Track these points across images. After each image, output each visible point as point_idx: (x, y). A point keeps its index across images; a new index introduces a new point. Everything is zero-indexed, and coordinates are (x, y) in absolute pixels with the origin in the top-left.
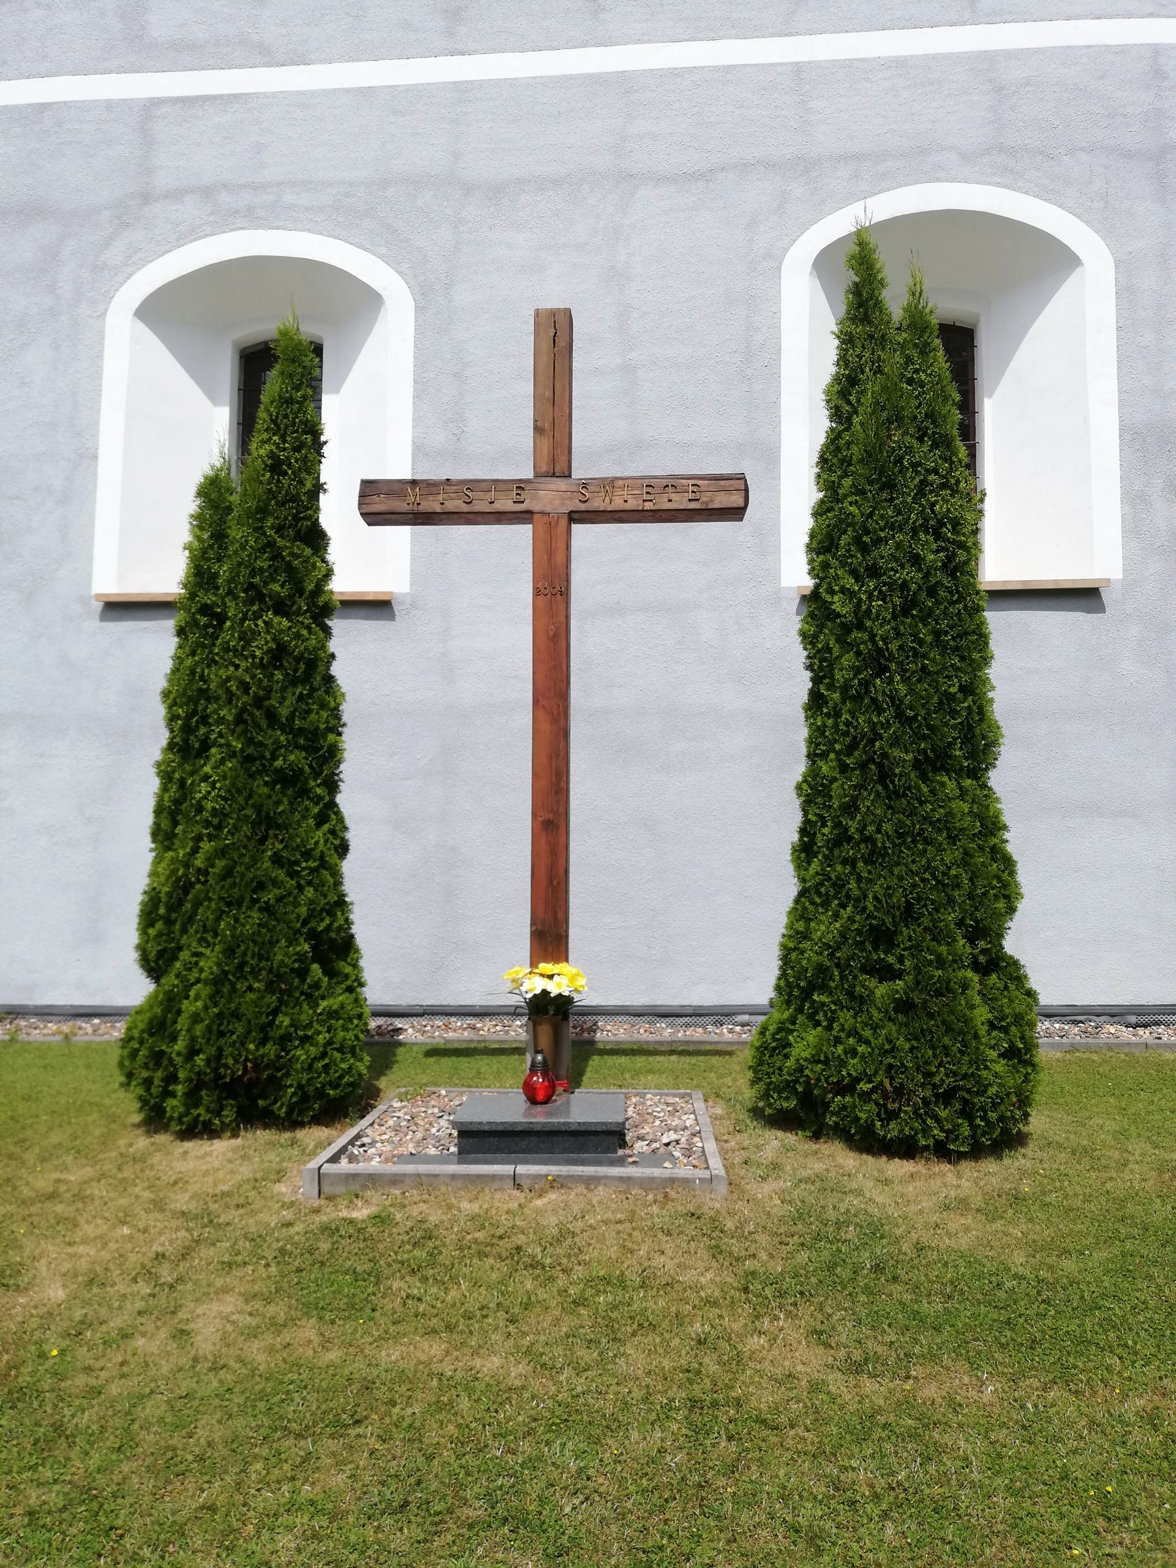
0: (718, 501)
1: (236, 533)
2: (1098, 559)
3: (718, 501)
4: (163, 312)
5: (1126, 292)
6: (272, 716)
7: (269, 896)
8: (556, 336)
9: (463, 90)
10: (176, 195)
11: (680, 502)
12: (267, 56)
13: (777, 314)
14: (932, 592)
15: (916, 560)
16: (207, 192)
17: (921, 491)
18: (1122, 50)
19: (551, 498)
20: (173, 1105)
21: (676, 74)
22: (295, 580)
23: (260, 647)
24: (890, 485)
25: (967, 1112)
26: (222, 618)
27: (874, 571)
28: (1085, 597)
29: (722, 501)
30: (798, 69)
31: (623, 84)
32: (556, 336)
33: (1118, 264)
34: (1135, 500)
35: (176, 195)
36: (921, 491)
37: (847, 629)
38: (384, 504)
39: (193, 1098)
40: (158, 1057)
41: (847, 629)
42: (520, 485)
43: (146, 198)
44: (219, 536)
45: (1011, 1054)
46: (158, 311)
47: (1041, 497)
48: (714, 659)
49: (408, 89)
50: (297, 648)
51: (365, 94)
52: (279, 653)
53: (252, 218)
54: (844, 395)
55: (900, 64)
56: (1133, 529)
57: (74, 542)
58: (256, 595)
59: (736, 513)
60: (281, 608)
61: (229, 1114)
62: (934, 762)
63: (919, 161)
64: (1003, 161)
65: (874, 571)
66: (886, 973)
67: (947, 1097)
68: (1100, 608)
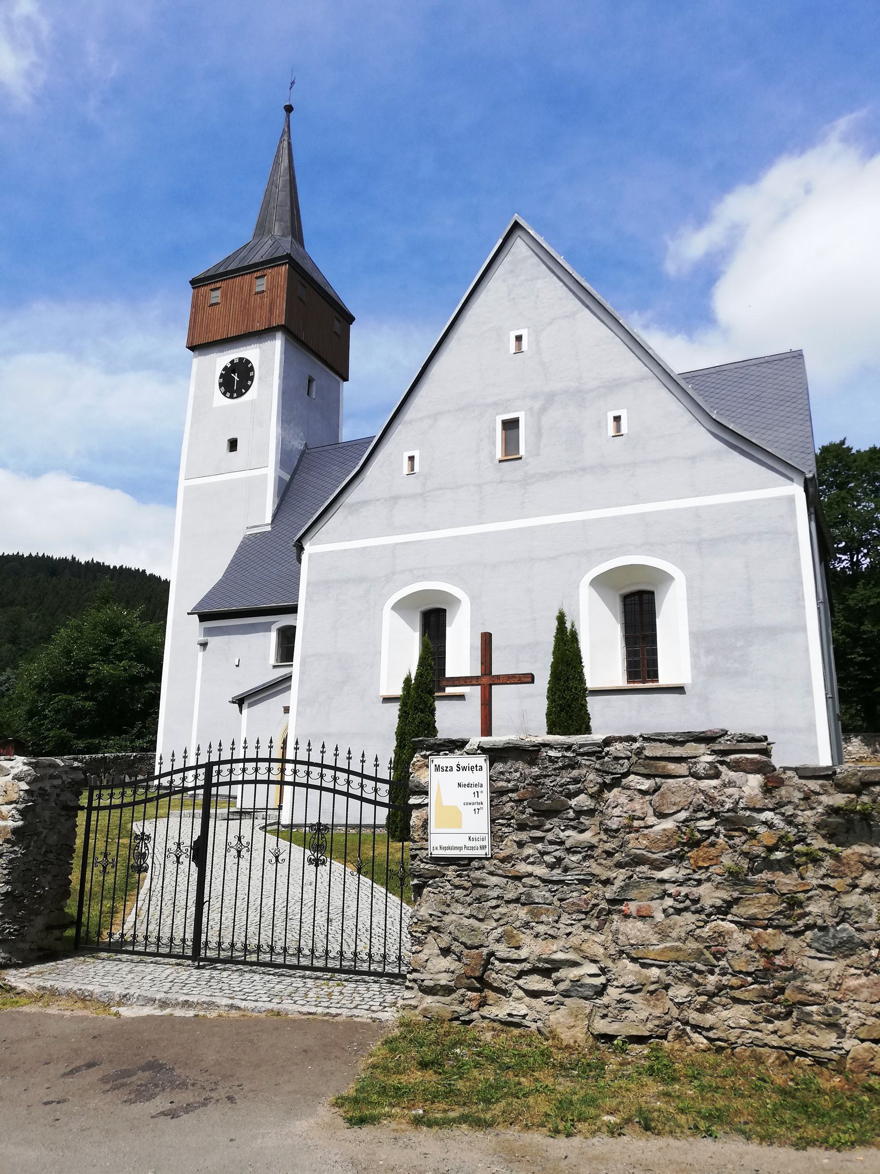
0: (529, 679)
1: (412, 693)
3: (529, 679)
4: (400, 607)
5: (690, 588)
9: (483, 535)
12: (427, 528)
13: (578, 600)
14: (569, 706)
15: (564, 698)
18: (686, 509)
19: (485, 680)
21: (547, 526)
22: (425, 704)
28: (679, 690)
31: (531, 530)
33: (687, 579)
34: (695, 656)
40: (394, 822)
42: (477, 677)
43: (394, 573)
44: (408, 693)
46: (398, 607)
50: (425, 721)
52: (421, 722)
56: (695, 666)
58: (416, 708)
59: (533, 682)
60: (422, 711)
63: (622, 550)
64: (649, 547)
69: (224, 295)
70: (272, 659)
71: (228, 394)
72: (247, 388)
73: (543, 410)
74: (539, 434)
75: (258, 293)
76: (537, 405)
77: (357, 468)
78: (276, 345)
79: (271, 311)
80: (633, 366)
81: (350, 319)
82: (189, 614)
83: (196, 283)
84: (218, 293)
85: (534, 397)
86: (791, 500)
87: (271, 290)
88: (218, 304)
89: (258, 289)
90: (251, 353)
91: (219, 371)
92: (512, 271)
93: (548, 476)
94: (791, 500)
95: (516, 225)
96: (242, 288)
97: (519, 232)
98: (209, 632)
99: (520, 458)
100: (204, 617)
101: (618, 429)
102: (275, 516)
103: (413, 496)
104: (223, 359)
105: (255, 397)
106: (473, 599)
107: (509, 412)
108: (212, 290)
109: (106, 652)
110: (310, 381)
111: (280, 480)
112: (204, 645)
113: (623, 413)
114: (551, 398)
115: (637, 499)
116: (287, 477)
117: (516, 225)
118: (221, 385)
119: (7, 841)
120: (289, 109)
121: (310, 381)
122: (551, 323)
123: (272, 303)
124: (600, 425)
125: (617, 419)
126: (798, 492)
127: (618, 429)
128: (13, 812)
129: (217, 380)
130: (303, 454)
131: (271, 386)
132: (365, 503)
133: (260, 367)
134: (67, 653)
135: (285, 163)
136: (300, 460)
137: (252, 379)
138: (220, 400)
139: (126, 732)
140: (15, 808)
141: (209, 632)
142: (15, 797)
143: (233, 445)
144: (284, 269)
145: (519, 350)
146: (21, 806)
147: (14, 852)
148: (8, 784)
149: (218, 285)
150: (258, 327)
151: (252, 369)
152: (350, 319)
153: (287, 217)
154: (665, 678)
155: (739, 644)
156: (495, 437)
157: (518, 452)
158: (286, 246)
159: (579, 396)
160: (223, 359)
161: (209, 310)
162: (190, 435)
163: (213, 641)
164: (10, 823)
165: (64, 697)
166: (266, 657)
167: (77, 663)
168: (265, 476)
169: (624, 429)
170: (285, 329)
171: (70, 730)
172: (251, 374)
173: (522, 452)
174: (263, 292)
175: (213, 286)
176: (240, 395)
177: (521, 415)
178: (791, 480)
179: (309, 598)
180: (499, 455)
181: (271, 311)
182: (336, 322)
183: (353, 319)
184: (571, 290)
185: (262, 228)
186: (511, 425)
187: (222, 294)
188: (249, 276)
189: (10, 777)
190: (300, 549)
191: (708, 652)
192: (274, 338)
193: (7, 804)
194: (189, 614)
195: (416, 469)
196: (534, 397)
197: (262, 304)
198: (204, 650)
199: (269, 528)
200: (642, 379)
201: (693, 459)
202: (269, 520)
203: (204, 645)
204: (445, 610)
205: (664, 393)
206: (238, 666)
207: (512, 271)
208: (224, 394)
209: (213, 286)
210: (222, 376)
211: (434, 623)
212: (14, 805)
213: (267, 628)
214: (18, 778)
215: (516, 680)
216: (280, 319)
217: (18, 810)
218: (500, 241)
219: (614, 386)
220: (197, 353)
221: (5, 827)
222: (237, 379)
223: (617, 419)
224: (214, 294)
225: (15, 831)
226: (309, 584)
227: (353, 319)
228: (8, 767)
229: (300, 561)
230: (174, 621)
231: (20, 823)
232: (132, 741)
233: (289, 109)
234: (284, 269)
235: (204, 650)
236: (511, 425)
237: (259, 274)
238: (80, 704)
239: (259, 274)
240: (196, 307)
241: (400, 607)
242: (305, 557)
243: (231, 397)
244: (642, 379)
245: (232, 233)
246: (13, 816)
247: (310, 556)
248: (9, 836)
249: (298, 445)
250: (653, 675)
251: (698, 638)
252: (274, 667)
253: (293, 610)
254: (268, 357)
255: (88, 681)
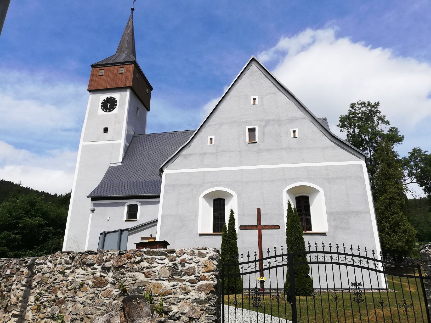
0: (277, 227)
2: (324, 229)
3: (277, 227)
4: (206, 197)
5: (326, 196)
6: (233, 251)
7: (233, 269)
8: (259, 210)
9: (242, 170)
10: (207, 183)
11: (273, 228)
15: (296, 235)
16: (211, 182)
17: (296, 228)
20: (225, 291)
21: (268, 169)
23: (231, 243)
24: (293, 228)
25: (304, 291)
26: (227, 240)
27: (292, 236)
28: (324, 234)
29: (277, 228)
30: (283, 168)
32: (259, 210)
34: (329, 221)
35: (207, 183)
36: (296, 228)
37: (290, 242)
38: (242, 228)
39: (227, 290)
41: (290, 242)
42: (256, 226)
43: (204, 183)
45: (309, 286)
46: (205, 197)
47: (319, 219)
48: (277, 241)
49: (235, 170)
51: (230, 171)
53: (217, 186)
54: (288, 217)
55: (295, 168)
56: (329, 225)
57: (196, 226)
61: (231, 292)
62: (300, 255)
65: (292, 236)
66: (296, 277)
67: (302, 289)
68: (326, 235)
69: (106, 72)
70: (125, 217)
71: (105, 110)
72: (114, 109)
73: (265, 126)
74: (264, 134)
75: (120, 73)
76: (263, 124)
77: (188, 141)
78: (127, 94)
79: (126, 81)
80: (299, 113)
81: (151, 89)
82: (87, 197)
83: (93, 66)
84: (103, 71)
85: (261, 121)
86: (361, 166)
87: (126, 73)
88: (102, 75)
89: (121, 72)
90: (116, 96)
91: (101, 100)
92: (251, 75)
93: (268, 150)
94: (361, 166)
95: (253, 59)
96: (114, 71)
97: (254, 62)
98: (95, 205)
99: (256, 143)
100: (93, 199)
101: (294, 135)
102: (123, 160)
103: (212, 154)
104: (103, 97)
105: (117, 112)
106: (239, 196)
107: (251, 125)
108: (100, 70)
109: (27, 213)
110: (138, 109)
111: (125, 145)
112: (93, 211)
113: (297, 130)
114: (268, 122)
115: (303, 161)
116: (128, 145)
117: (253, 59)
118: (102, 106)
119: (211, 292)
120: (133, 9)
121: (138, 109)
122: (267, 95)
123: (127, 78)
124: (288, 133)
125: (294, 132)
126: (363, 163)
127: (294, 135)
128: (213, 276)
129: (100, 104)
130: (133, 136)
131: (124, 109)
132: (191, 155)
133: (120, 101)
134: (10, 213)
135: (131, 28)
136: (132, 139)
137: (116, 105)
138: (101, 112)
139: (35, 248)
140: (213, 274)
141: (95, 205)
142: (213, 268)
143: (106, 130)
144: (132, 66)
145: (254, 103)
146: (217, 273)
147: (215, 298)
148: (207, 261)
149: (103, 68)
150: (120, 86)
151: (116, 101)
152: (151, 89)
153: (131, 47)
154: (314, 229)
155: (346, 217)
156: (246, 134)
157: (255, 140)
158: (132, 58)
159: (279, 122)
160: (103, 97)
161: (99, 77)
162: (87, 124)
163: (97, 209)
164: (211, 282)
165: (7, 232)
166: (122, 217)
167: (14, 217)
168: (120, 143)
169: (297, 135)
170: (131, 88)
171: (8, 247)
172: (116, 103)
173: (257, 140)
174: (123, 73)
175: (101, 68)
176: (110, 111)
177: (256, 127)
178: (361, 159)
179: (165, 191)
180: (248, 141)
181: (126, 81)
182: (147, 89)
183: (152, 89)
184: (274, 84)
185: (120, 50)
186: (252, 130)
187: (105, 71)
188: (117, 67)
189: (207, 258)
190: (161, 171)
191: (334, 220)
192: (126, 91)
193: (207, 272)
194: (87, 197)
195: (213, 143)
196: (261, 121)
197: (122, 78)
198: (93, 213)
199: (120, 164)
200: (303, 118)
201: (324, 148)
202: (120, 161)
203: (93, 211)
204: (224, 200)
205: (312, 124)
206: (108, 220)
207: (251, 75)
208: (103, 110)
209: (101, 68)
210: (102, 103)
211: (219, 204)
212: (212, 273)
213: (123, 205)
214: (210, 258)
215: (273, 228)
216: (130, 83)
217: (215, 275)
218: (247, 64)
219: (292, 120)
220: (92, 93)
221: (210, 284)
222: (109, 105)
223: (294, 132)
224: (101, 71)
225: (215, 287)
226: (165, 186)
227: (152, 89)
228: (205, 253)
229: (161, 177)
230: (74, 201)
231: (216, 282)
232: (37, 253)
233: (133, 9)
234: (132, 66)
235: (93, 213)
236: (252, 130)
237: (121, 66)
238: (13, 236)
239: (121, 66)
240: (92, 75)
241: (206, 197)
242: (164, 175)
243: (106, 111)
244: (303, 118)
245: (109, 50)
246: (212, 278)
247: (166, 174)
248: (213, 289)
249: (132, 133)
250: (310, 228)
251: (330, 214)
252: (126, 221)
253: (158, 197)
254: (123, 98)
255: (20, 225)
